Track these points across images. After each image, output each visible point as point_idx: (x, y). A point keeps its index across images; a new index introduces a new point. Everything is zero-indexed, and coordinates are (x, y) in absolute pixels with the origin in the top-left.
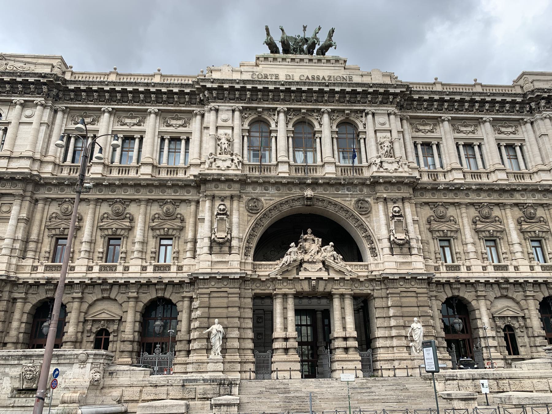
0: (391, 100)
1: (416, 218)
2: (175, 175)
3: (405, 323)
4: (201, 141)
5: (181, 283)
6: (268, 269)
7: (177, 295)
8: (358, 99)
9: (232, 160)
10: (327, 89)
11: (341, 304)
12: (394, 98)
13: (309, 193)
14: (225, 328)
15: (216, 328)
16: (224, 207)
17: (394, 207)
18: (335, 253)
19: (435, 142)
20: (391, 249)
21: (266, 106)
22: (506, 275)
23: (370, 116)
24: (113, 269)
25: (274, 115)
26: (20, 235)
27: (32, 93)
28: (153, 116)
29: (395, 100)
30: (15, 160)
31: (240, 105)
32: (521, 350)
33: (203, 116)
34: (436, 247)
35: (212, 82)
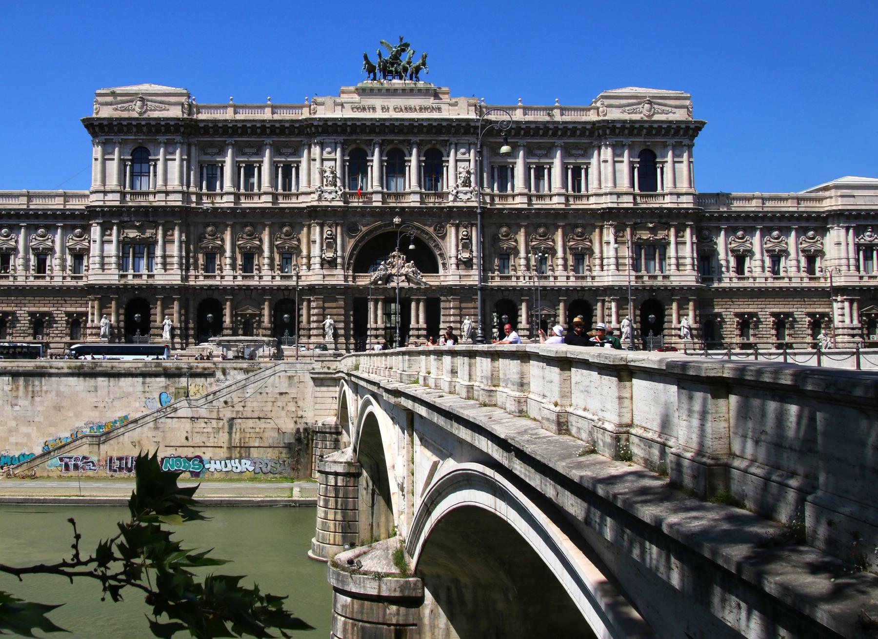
9: (336, 192)
13: (397, 220)
15: (328, 321)
20: (458, 265)
21: (364, 138)
27: (173, 133)
31: (341, 139)
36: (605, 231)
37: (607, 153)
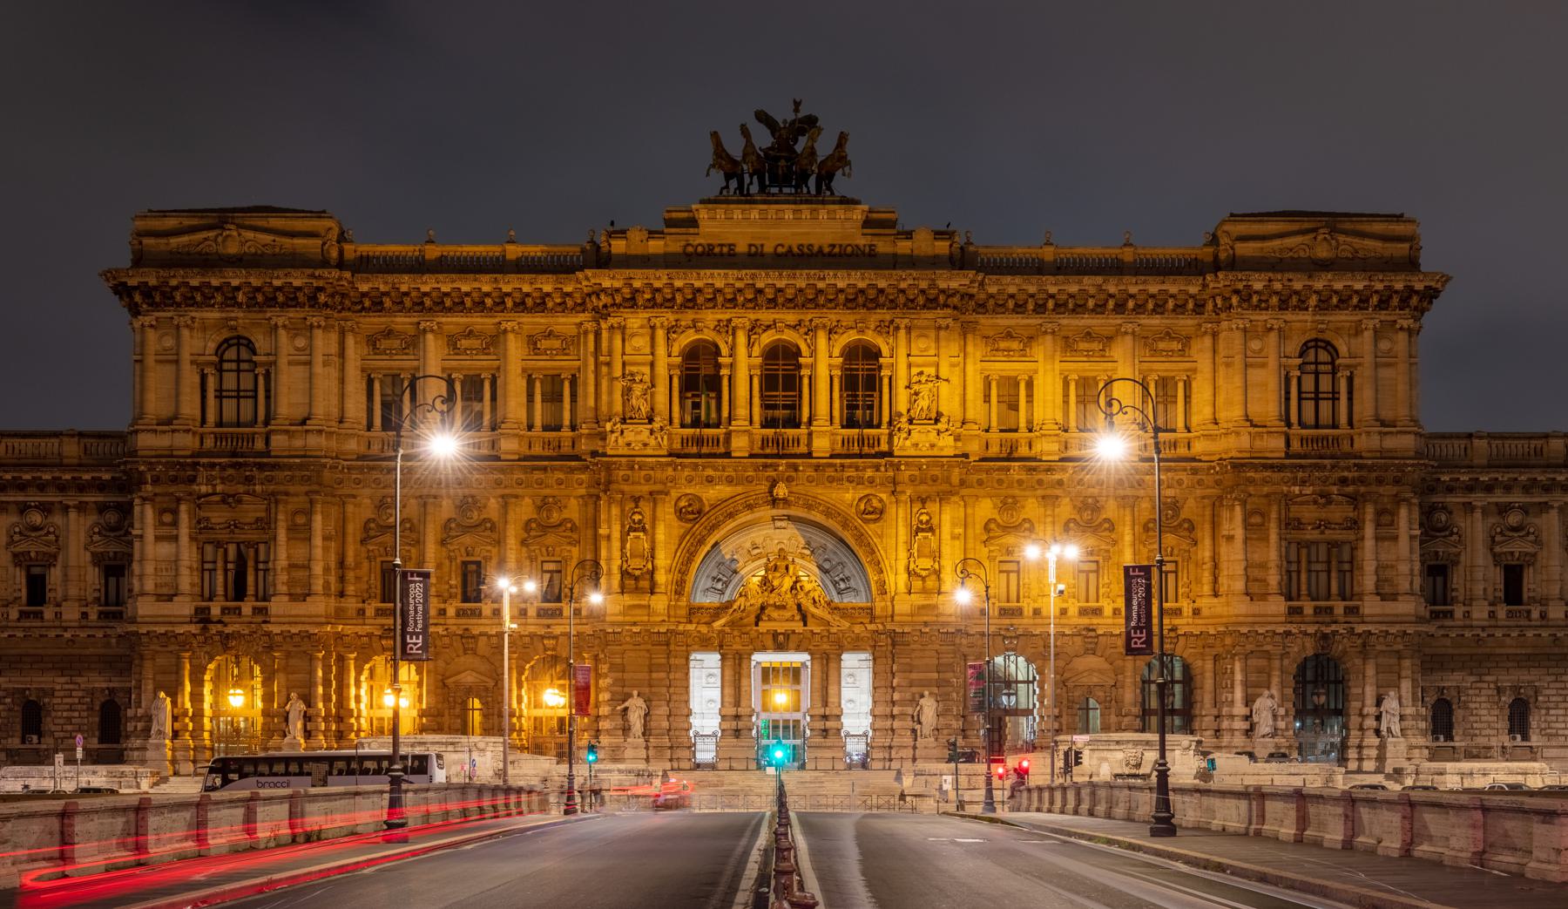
14: (648, 701)
19: (1023, 378)
36: (1225, 514)
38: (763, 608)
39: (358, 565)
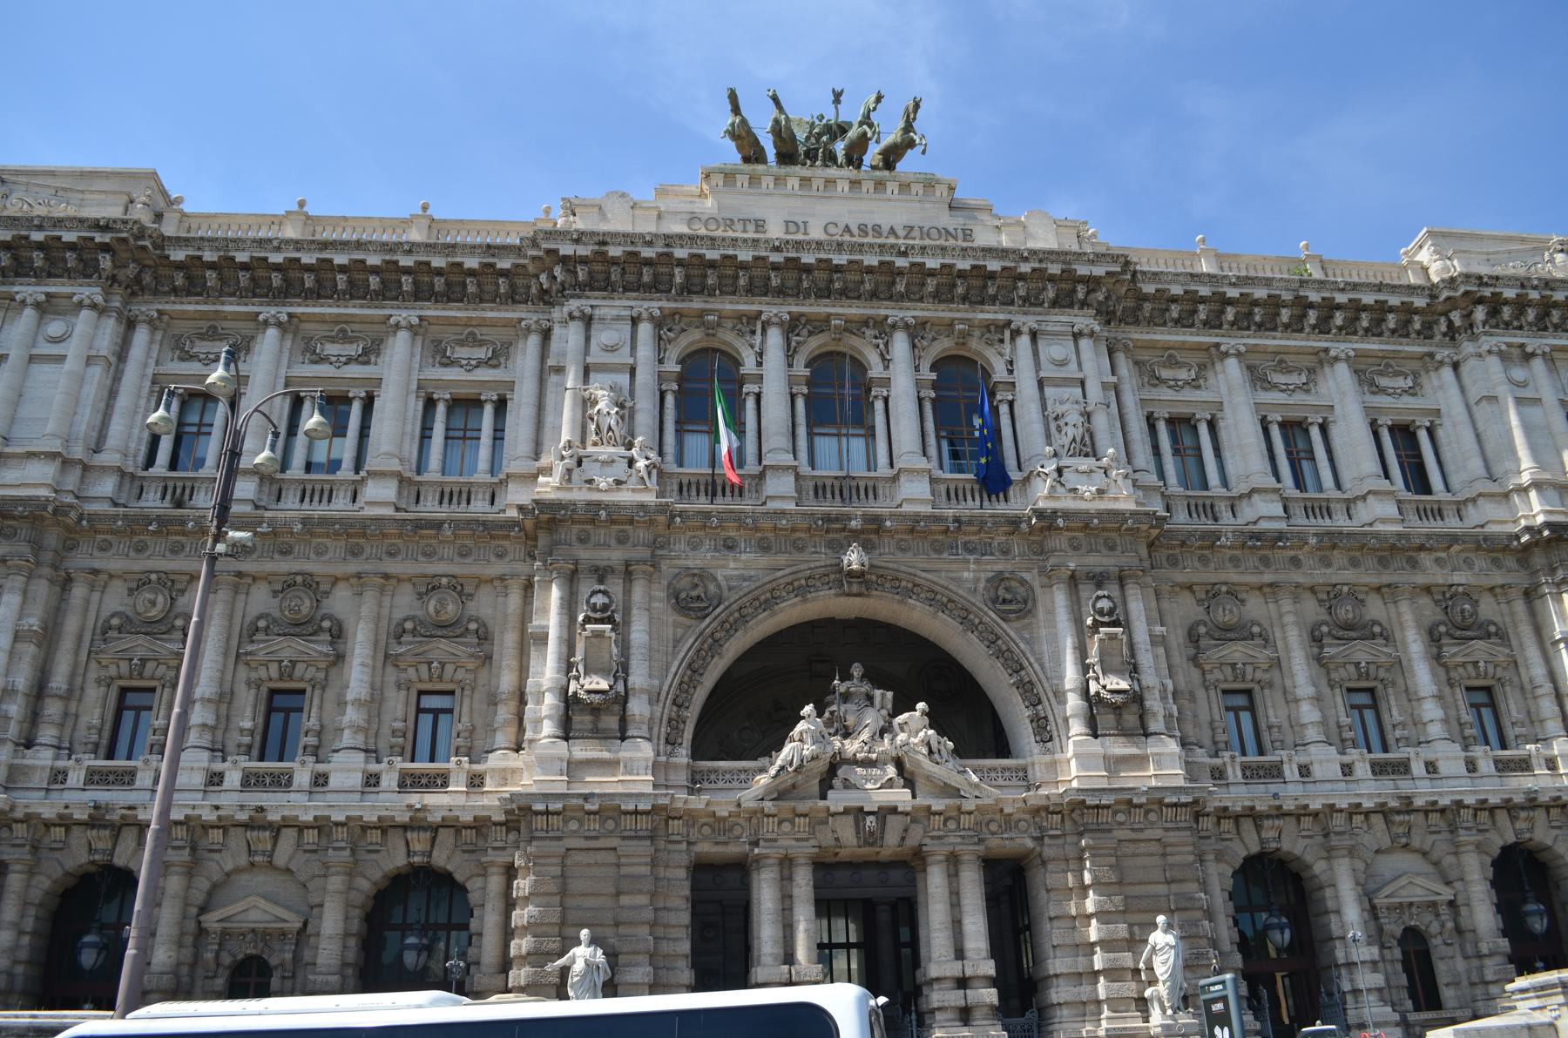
0: (1081, 296)
1: (1159, 629)
2: (464, 504)
3: (1131, 933)
4: (540, 407)
5: (481, 825)
6: (735, 783)
7: (466, 856)
8: (991, 291)
9: (631, 462)
10: (901, 262)
11: (950, 883)
12: (1088, 293)
13: (854, 558)
14: (612, 956)
16: (606, 600)
17: (1098, 598)
18: (931, 732)
21: (729, 307)
22: (1405, 787)
23: (1024, 341)
24: (282, 782)
25: (753, 332)
26: (22, 680)
27: (68, 273)
28: (403, 335)
29: (1092, 296)
30: (15, 461)
31: (655, 305)
32: (1447, 994)
33: (546, 335)
34: (1215, 710)
35: (577, 241)
37: (1486, 373)
38: (833, 769)
39: (72, 693)
